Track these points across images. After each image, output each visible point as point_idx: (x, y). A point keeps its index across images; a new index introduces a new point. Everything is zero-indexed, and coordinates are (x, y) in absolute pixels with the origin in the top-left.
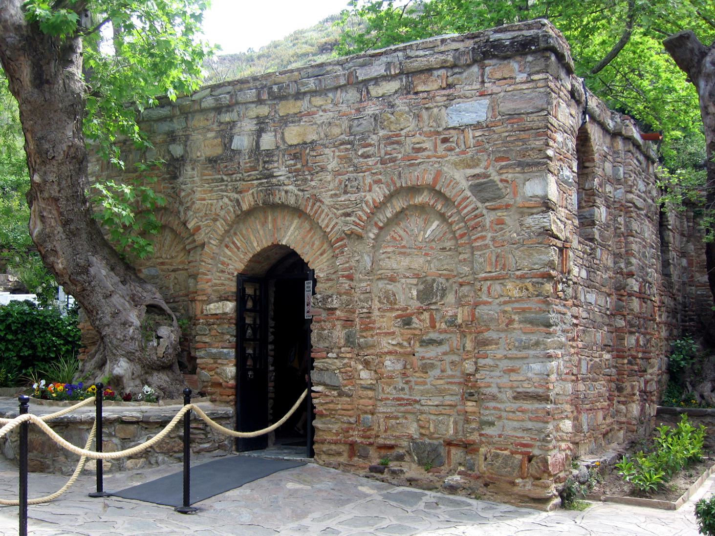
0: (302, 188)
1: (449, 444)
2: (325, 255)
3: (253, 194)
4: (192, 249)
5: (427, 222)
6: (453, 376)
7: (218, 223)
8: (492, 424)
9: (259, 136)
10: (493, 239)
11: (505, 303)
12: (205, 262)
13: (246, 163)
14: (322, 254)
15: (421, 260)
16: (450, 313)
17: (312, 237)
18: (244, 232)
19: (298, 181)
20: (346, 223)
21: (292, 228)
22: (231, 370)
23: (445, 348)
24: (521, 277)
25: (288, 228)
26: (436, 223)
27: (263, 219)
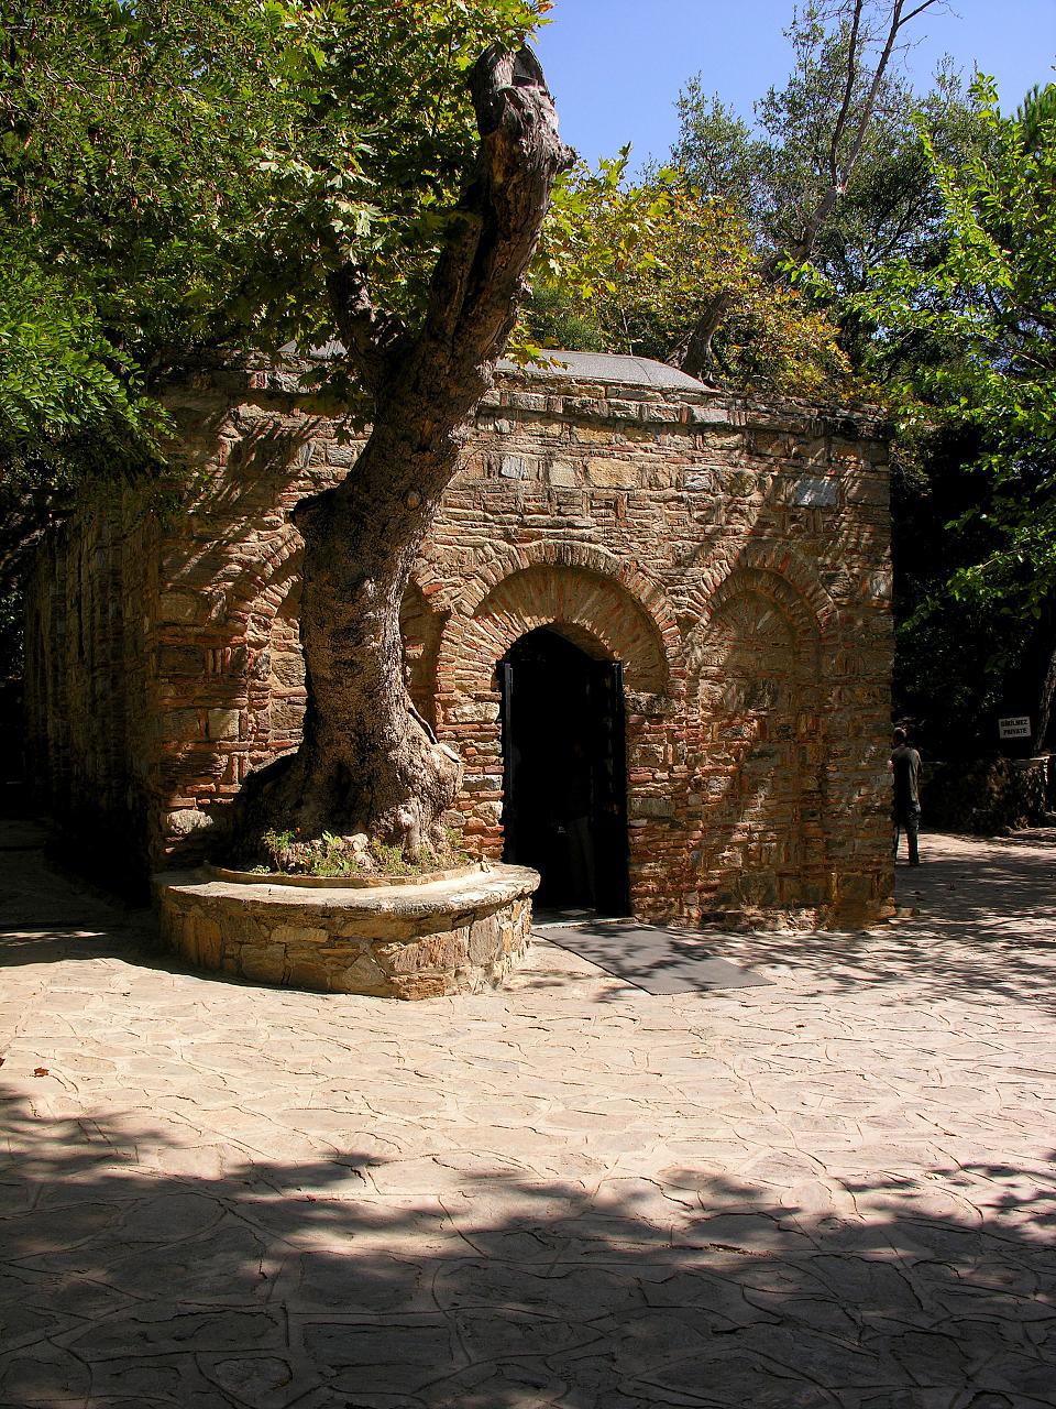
0: (618, 549)
1: (781, 875)
2: (638, 643)
3: (540, 546)
4: (413, 617)
5: (759, 612)
6: (786, 794)
7: (473, 582)
8: (841, 844)
9: (548, 465)
10: (844, 639)
11: (856, 709)
12: (452, 641)
13: (529, 500)
14: (635, 641)
15: (752, 657)
16: (782, 721)
17: (620, 616)
18: (509, 599)
19: (612, 538)
20: (679, 606)
21: (590, 601)
22: (499, 806)
23: (777, 760)
24: (871, 682)
25: (583, 602)
26: (768, 614)
27: (541, 583)
